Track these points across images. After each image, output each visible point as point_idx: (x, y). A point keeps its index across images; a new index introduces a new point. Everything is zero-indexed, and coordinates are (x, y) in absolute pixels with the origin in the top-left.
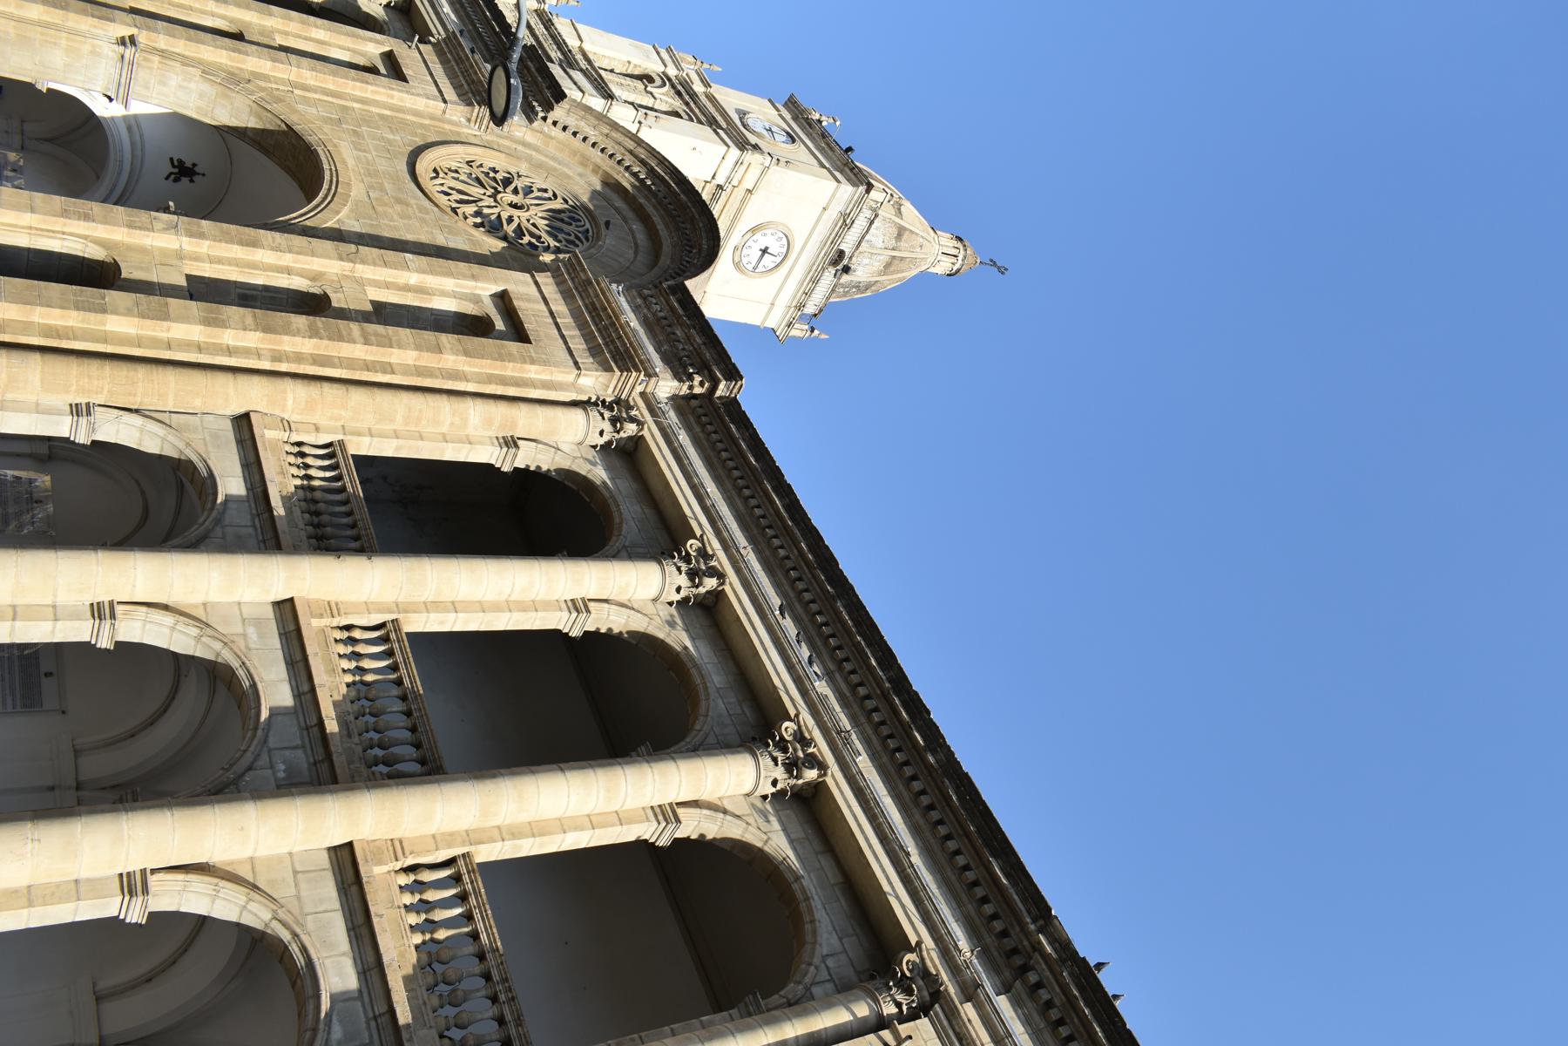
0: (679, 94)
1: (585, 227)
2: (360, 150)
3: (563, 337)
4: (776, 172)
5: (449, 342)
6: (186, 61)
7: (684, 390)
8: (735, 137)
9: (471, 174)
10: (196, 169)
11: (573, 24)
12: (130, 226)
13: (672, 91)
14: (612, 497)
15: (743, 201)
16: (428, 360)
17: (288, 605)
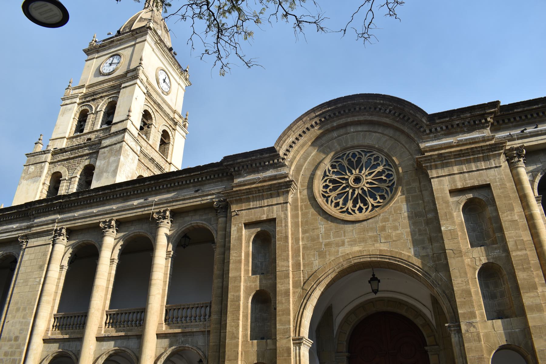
0: (93, 100)
2: (343, 244)
5: (507, 217)
8: (128, 79)
12: (480, 341)
15: (150, 84)
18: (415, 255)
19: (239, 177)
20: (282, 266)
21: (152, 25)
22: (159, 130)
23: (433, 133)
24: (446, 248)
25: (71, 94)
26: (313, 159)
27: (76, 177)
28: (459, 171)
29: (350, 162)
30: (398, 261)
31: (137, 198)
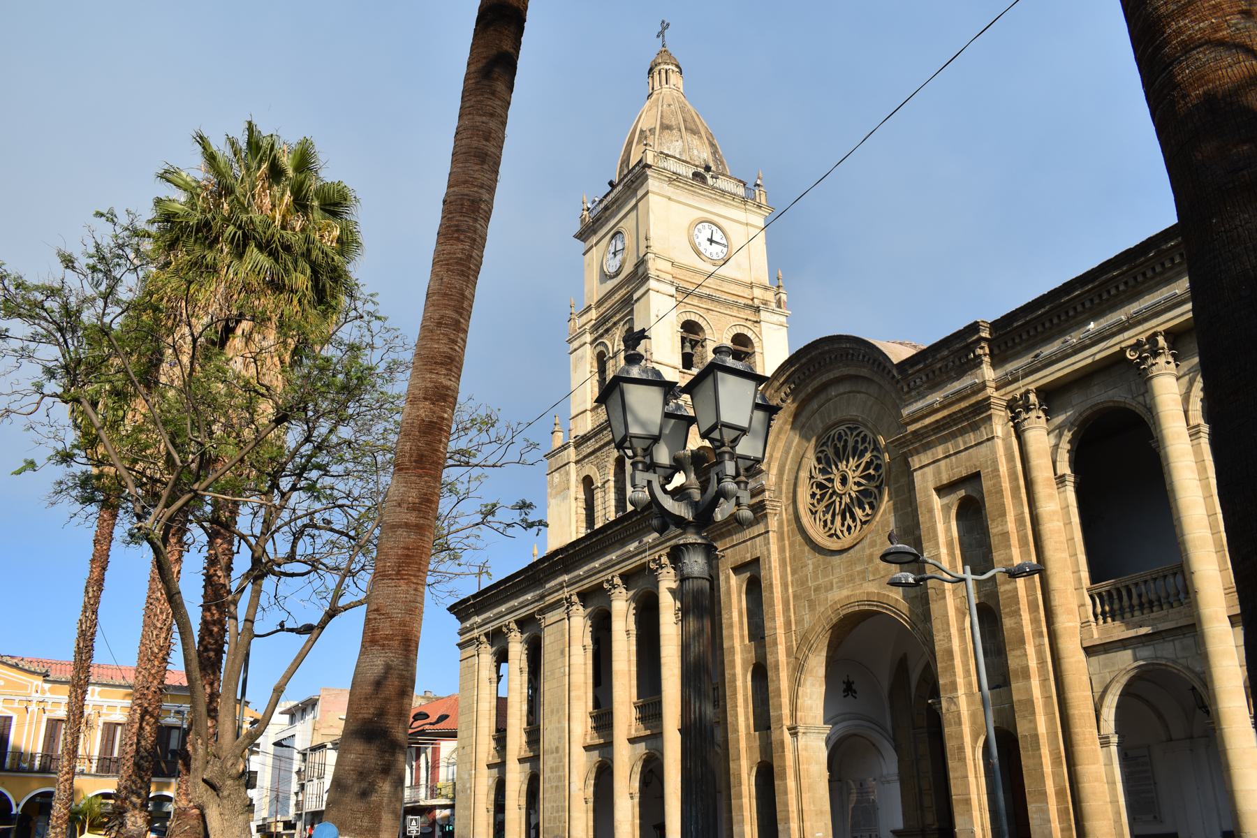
0: (607, 331)
2: (832, 589)
3: (966, 449)
4: (656, 245)
7: (987, 359)
10: (846, 680)
11: (573, 418)
12: (960, 723)
13: (606, 336)
14: (1091, 407)
15: (681, 267)
17: (1233, 619)
18: (904, 598)
20: (771, 628)
24: (929, 586)
25: (578, 326)
26: (797, 452)
28: (946, 452)
30: (887, 609)
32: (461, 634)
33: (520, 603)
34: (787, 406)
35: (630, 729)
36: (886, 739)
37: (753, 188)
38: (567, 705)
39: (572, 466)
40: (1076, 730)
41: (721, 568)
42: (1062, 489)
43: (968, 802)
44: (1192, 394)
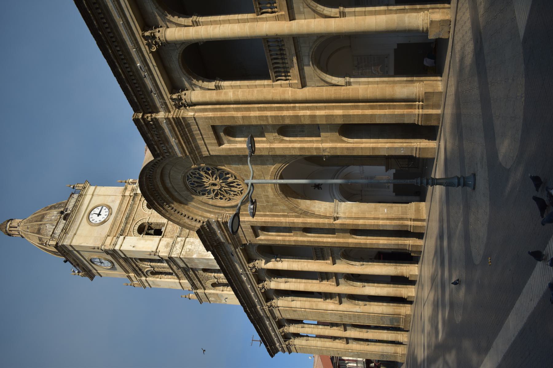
0: (140, 270)
1: (188, 181)
2: (267, 195)
3: (200, 130)
4: (98, 244)
5: (239, 121)
6: (320, 216)
7: (154, 115)
9: (229, 195)
10: (314, 187)
11: (183, 288)
12: (336, 148)
13: (143, 270)
15: (110, 232)
16: (246, 114)
17: (291, 19)
19: (220, 240)
21: (54, 243)
22: (150, 213)
23: (168, 150)
24: (268, 154)
26: (199, 204)
27: (214, 276)
29: (201, 186)
30: (278, 173)
31: (241, 277)
32: (284, 352)
33: (270, 327)
34: (175, 206)
35: (332, 285)
36: (343, 170)
37: (75, 189)
38: (320, 311)
39: (206, 291)
40: (342, 97)
41: (256, 242)
42: (223, 88)
43: (373, 149)
44: (176, 22)
